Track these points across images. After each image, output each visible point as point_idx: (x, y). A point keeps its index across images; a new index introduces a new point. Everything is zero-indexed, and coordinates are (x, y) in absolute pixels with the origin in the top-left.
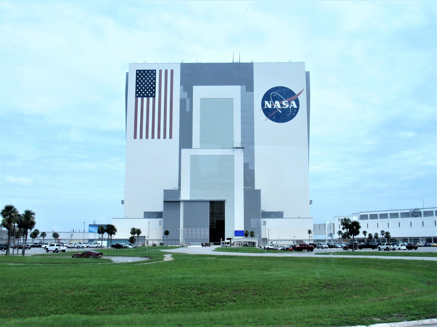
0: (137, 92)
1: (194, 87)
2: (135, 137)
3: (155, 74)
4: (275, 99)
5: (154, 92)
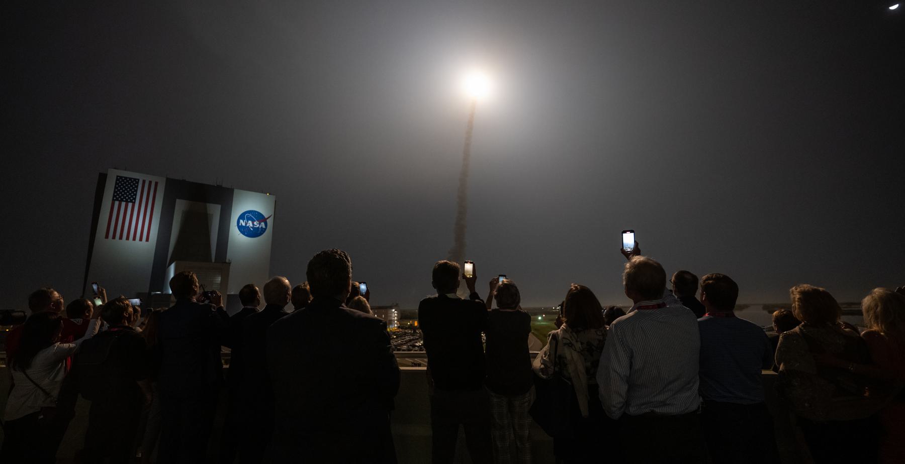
0: (114, 196)
1: (178, 201)
2: (107, 237)
3: (138, 183)
4: (249, 219)
5: (135, 199)
